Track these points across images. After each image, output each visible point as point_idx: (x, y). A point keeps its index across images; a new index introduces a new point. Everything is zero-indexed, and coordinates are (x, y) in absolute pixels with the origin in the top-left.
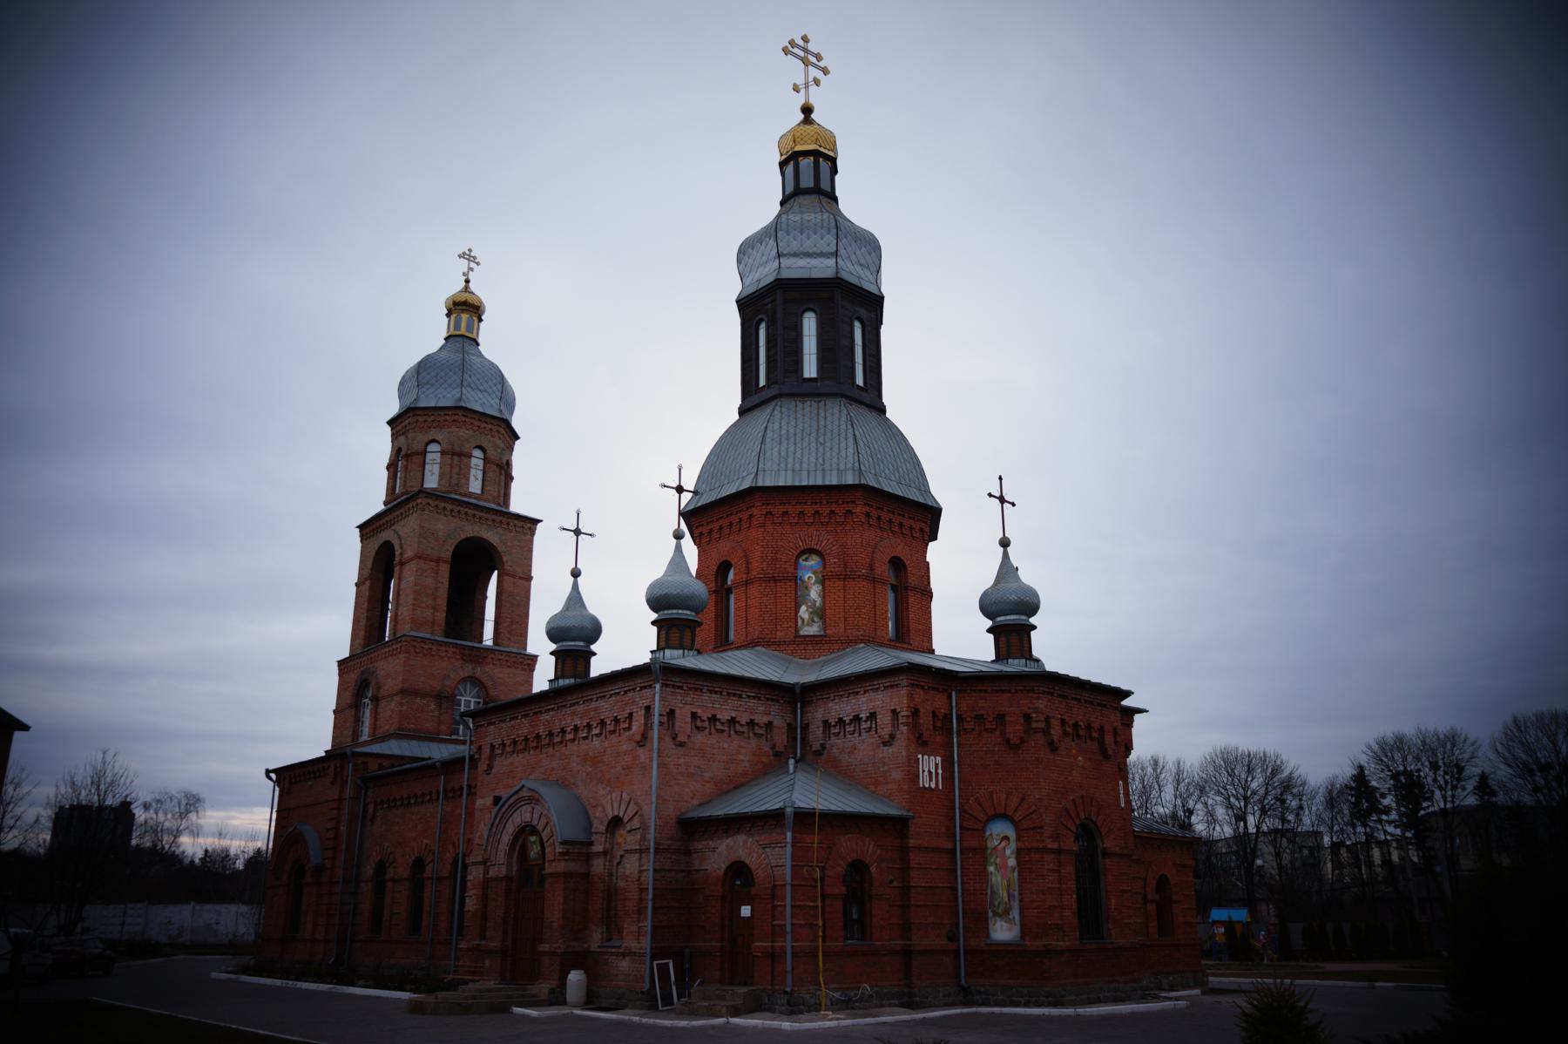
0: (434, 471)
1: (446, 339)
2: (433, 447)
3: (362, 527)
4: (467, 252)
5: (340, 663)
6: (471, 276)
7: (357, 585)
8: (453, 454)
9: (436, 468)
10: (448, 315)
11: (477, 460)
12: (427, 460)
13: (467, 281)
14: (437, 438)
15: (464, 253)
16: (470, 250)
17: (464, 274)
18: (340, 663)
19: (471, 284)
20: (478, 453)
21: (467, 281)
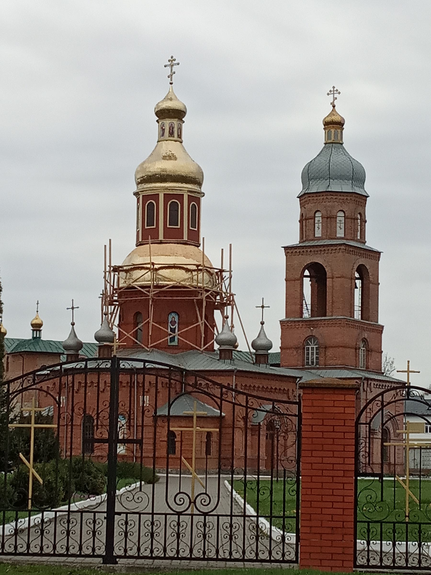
0: (341, 227)
1: (325, 144)
2: (341, 214)
3: (286, 248)
4: (332, 90)
5: (282, 322)
6: (335, 103)
7: (286, 281)
8: (352, 218)
9: (342, 226)
10: (325, 129)
11: (359, 221)
12: (338, 222)
13: (334, 107)
14: (344, 210)
15: (331, 91)
16: (334, 87)
17: (331, 103)
18: (282, 322)
19: (336, 108)
20: (359, 216)
21: (334, 107)
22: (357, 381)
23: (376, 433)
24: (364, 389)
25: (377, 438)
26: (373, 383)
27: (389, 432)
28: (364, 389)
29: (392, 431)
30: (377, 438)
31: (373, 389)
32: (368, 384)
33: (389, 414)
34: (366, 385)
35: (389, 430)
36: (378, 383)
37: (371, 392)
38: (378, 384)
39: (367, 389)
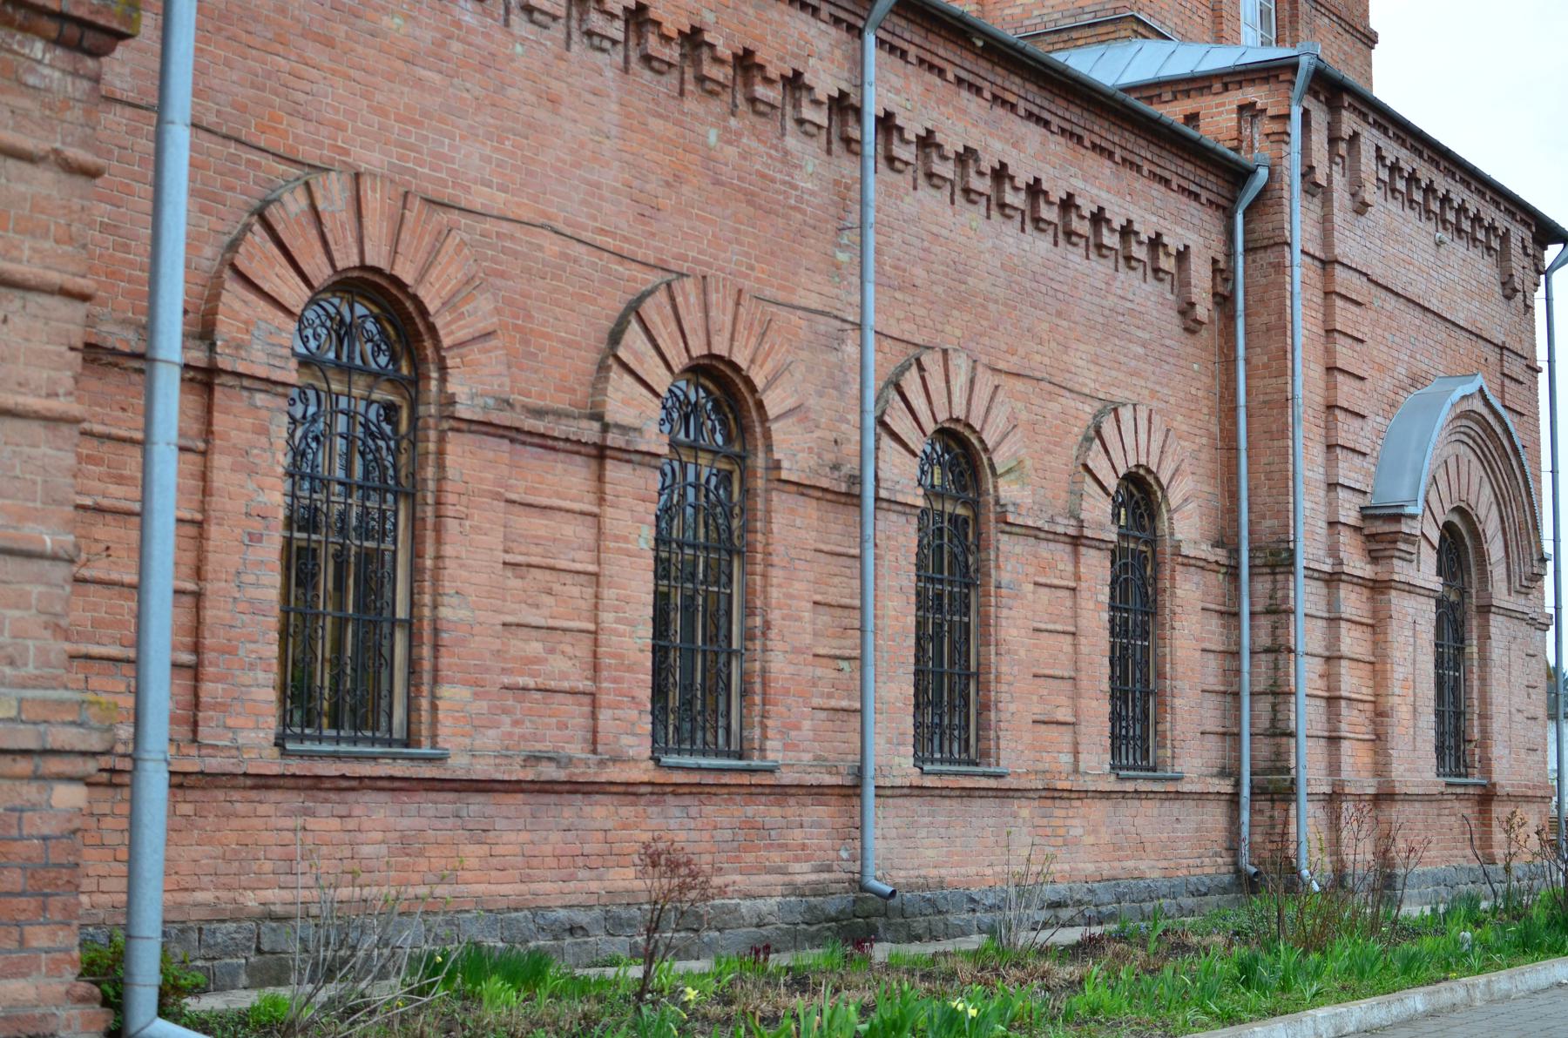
22: (1255, 94)
23: (1409, 538)
24: (1309, 169)
25: (1411, 589)
26: (1370, 138)
27: (1482, 558)
28: (1309, 169)
29: (1495, 550)
30: (1411, 589)
31: (1371, 194)
32: (1333, 140)
33: (1478, 405)
34: (1319, 139)
35: (1477, 536)
36: (1408, 161)
37: (1362, 208)
38: (1407, 168)
39: (1330, 181)
